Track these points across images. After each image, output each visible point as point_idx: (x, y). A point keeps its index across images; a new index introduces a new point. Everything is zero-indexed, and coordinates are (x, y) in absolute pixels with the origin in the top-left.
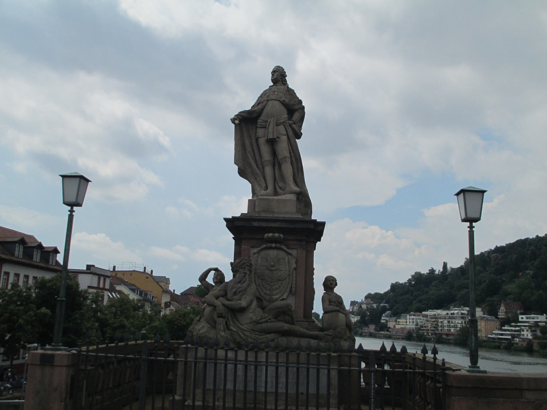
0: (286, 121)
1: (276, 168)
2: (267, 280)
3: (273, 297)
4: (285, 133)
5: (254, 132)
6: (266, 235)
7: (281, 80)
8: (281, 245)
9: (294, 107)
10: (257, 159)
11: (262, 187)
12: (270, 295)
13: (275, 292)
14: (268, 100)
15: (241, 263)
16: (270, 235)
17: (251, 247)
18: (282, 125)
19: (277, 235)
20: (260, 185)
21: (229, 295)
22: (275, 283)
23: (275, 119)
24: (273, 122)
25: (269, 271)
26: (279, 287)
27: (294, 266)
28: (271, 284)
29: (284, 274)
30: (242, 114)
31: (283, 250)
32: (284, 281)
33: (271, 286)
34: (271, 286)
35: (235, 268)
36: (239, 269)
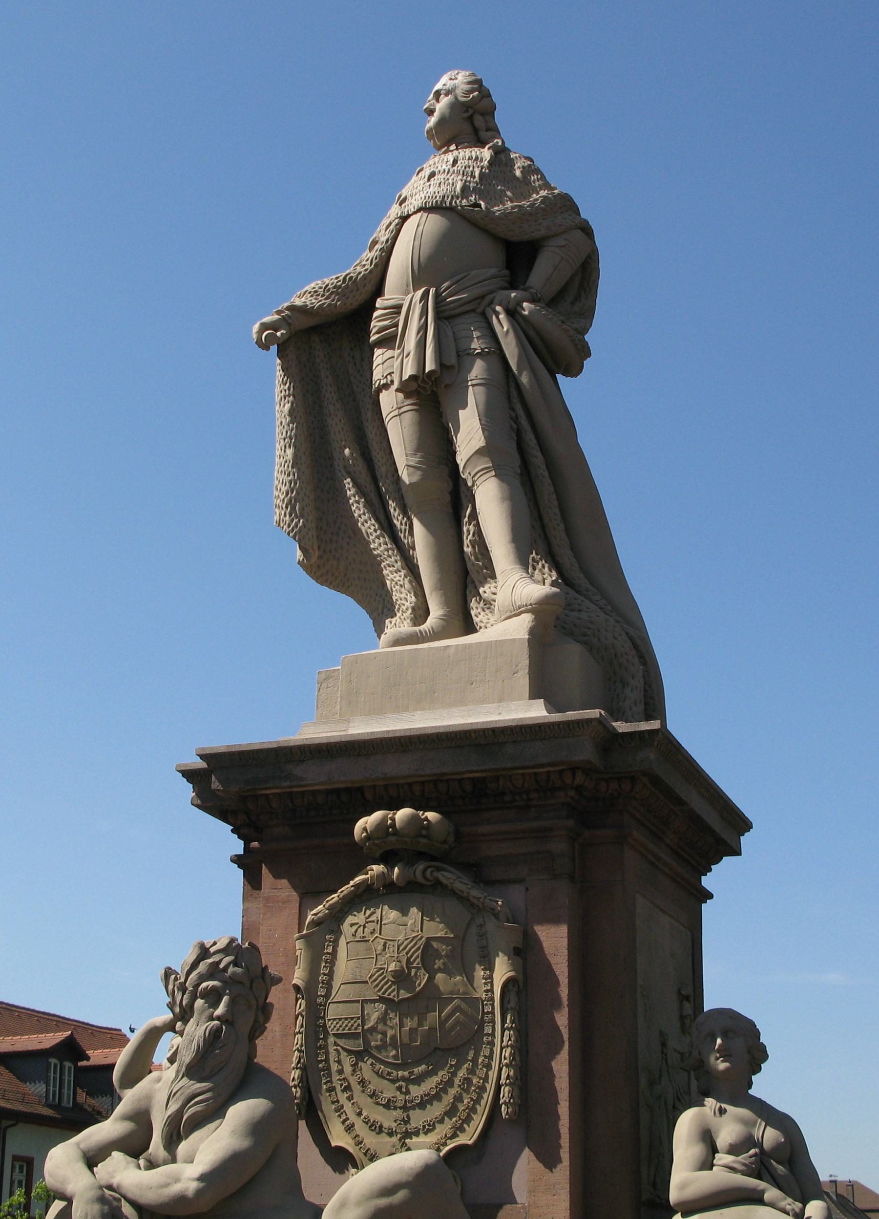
0: (492, 292)
8: (439, 869)
18: (474, 310)
19: (403, 814)
25: (382, 1007)
31: (454, 893)
35: (178, 997)
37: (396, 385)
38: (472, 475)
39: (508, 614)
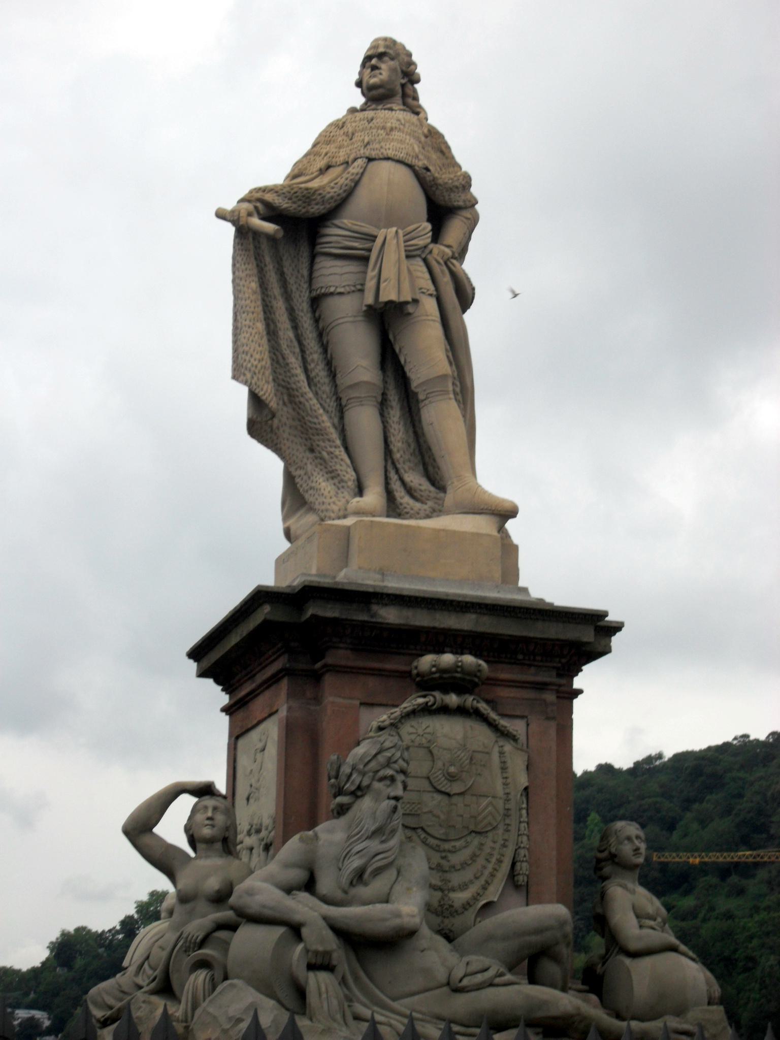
1: (395, 414)
2: (428, 830)
3: (453, 895)
4: (432, 288)
5: (305, 273)
6: (427, 661)
7: (400, 91)
9: (452, 195)
10: (313, 375)
11: (342, 481)
12: (441, 890)
13: (456, 879)
14: (370, 160)
15: (381, 759)
16: (448, 659)
17: (361, 704)
18: (419, 256)
20: (333, 475)
21: (326, 883)
22: (458, 844)
23: (401, 232)
24: (395, 241)
25: (438, 797)
26: (474, 857)
27: (523, 780)
28: (447, 846)
29: (490, 808)
30: (269, 197)
32: (490, 835)
33: (444, 854)
34: (444, 854)
36: (373, 779)
37: (369, 299)
38: (428, 391)
39: (465, 510)
